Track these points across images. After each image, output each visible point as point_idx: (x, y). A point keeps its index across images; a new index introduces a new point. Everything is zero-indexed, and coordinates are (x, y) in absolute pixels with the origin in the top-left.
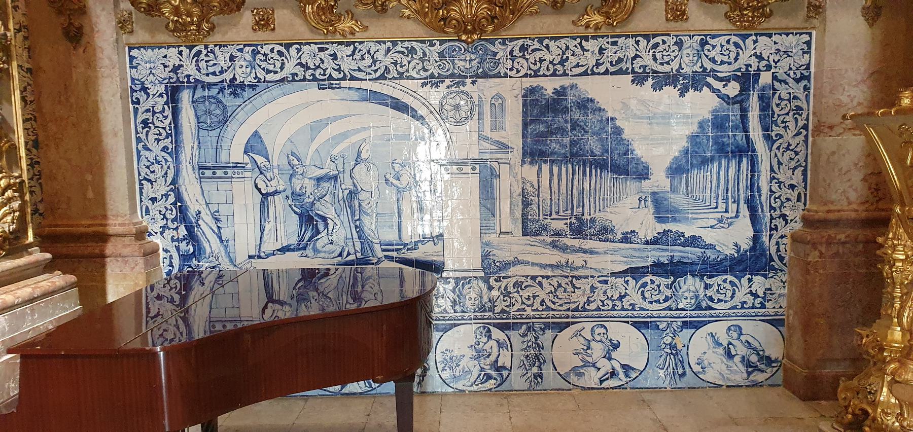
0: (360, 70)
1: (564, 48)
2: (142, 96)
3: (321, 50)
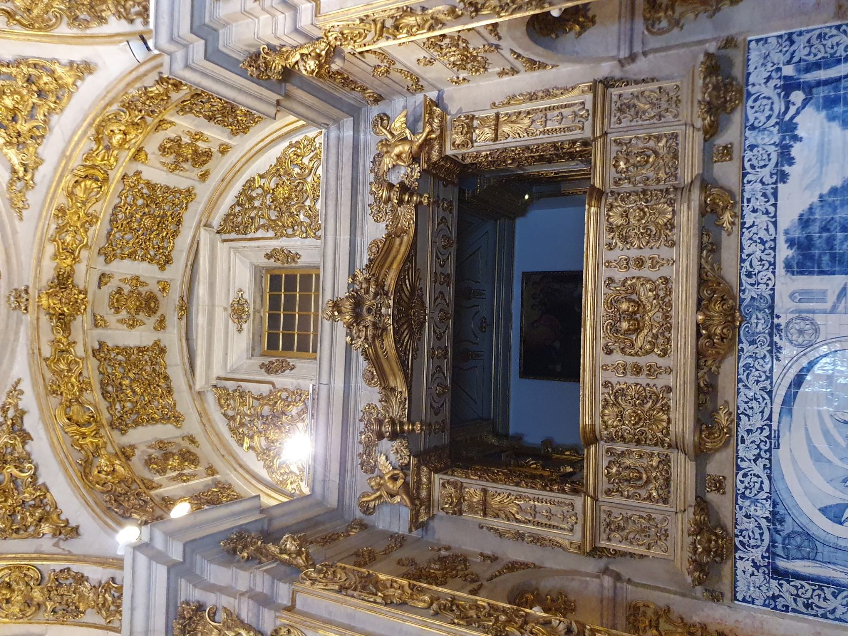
0: (762, 412)
1: (751, 242)
2: (780, 602)
3: (743, 441)
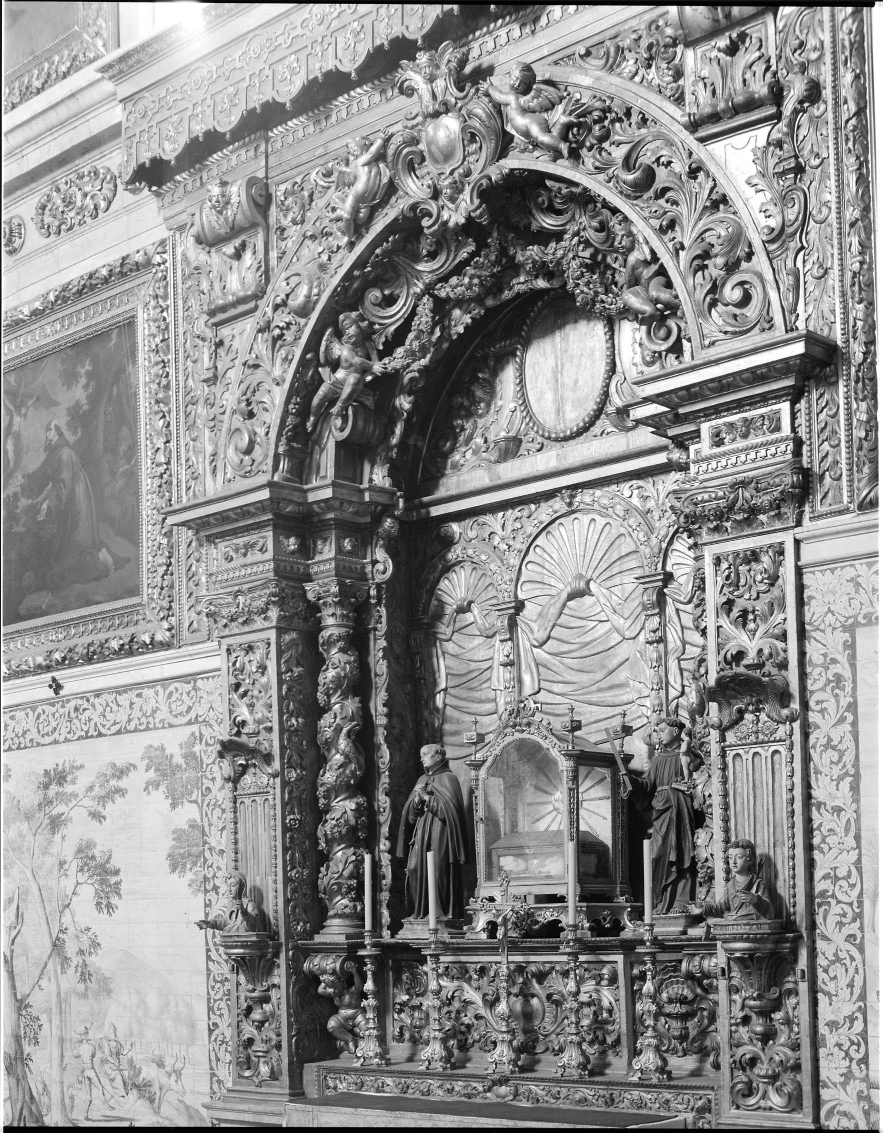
0: (851, 985)
